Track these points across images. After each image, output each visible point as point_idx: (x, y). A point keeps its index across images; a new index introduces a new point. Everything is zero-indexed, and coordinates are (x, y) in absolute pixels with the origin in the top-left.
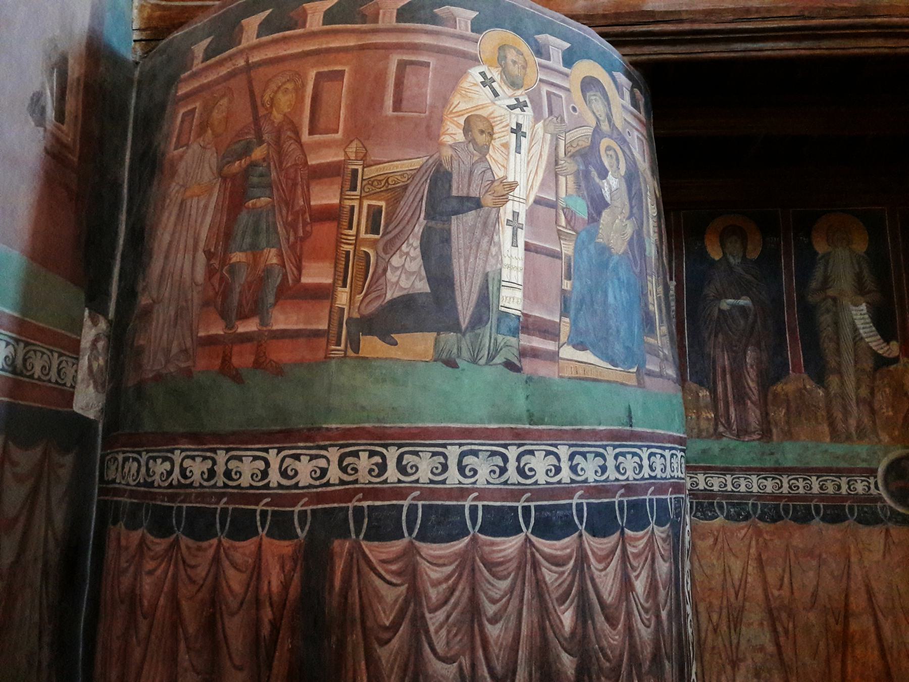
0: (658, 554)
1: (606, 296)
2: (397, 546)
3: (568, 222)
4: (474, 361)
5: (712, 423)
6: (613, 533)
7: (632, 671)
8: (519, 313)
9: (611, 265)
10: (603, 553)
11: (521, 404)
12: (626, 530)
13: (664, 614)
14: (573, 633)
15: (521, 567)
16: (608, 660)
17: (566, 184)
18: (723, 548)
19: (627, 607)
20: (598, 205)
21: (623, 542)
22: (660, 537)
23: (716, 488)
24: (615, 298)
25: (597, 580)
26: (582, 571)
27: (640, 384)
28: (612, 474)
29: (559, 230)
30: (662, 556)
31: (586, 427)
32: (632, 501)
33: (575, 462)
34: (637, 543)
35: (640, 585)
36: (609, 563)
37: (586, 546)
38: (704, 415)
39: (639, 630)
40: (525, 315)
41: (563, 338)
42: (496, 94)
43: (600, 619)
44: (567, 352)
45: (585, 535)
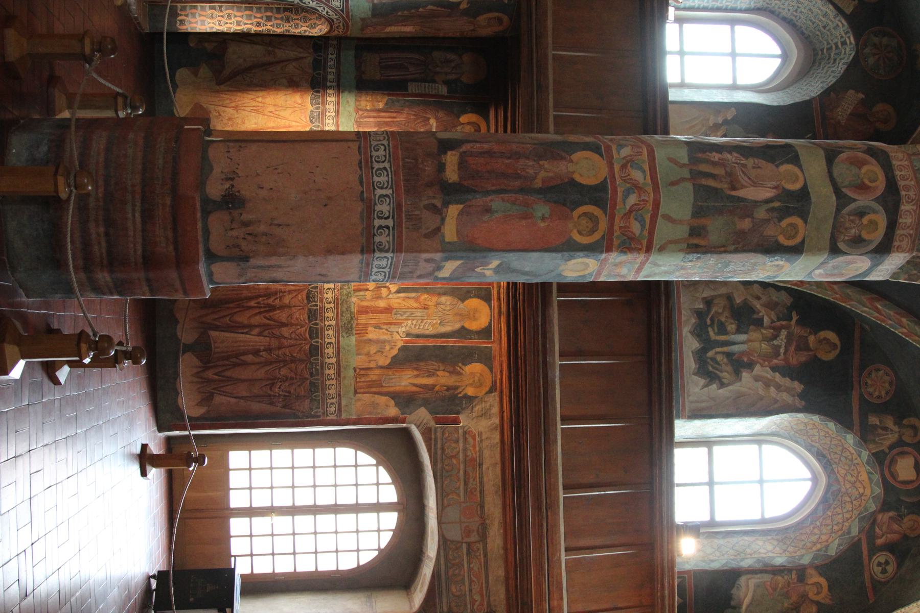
5: (364, 108)
18: (295, 107)
23: (328, 106)
38: (368, 104)
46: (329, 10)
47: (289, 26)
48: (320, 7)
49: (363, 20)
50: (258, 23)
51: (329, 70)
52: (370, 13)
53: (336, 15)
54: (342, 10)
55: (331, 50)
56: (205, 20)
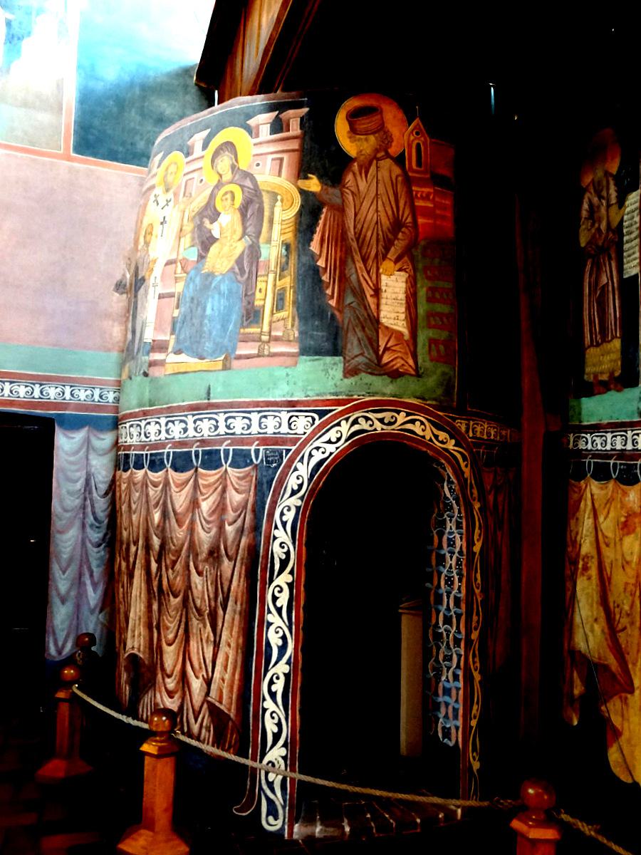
0: (230, 488)
1: (204, 310)
2: (120, 472)
3: (183, 268)
4: (135, 375)
6: (190, 470)
7: (189, 556)
8: (151, 341)
9: (213, 285)
10: (179, 482)
11: (147, 395)
12: (200, 470)
13: (230, 529)
14: (158, 526)
15: (142, 485)
16: (174, 545)
17: (186, 241)
19: (192, 516)
20: (206, 242)
21: (196, 476)
22: (235, 476)
24: (213, 309)
25: (174, 498)
26: (166, 491)
27: (226, 367)
28: (191, 433)
29: (176, 277)
30: (236, 490)
31: (175, 405)
32: (205, 450)
33: (168, 427)
34: (209, 478)
35: (206, 506)
36: (183, 489)
37: (170, 476)
39: (198, 533)
40: (154, 341)
41: (170, 350)
42: (158, 204)
43: (173, 521)
44: (172, 358)
45: (171, 472)
46: (325, 438)
47: (451, 521)
48: (311, 456)
49: (350, 372)
50: (446, 583)
51: (608, 447)
52: (328, 359)
53: (339, 424)
54: (321, 414)
55: (582, 446)
56: (444, 687)
